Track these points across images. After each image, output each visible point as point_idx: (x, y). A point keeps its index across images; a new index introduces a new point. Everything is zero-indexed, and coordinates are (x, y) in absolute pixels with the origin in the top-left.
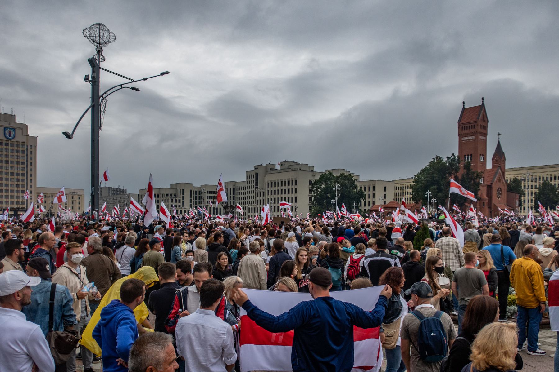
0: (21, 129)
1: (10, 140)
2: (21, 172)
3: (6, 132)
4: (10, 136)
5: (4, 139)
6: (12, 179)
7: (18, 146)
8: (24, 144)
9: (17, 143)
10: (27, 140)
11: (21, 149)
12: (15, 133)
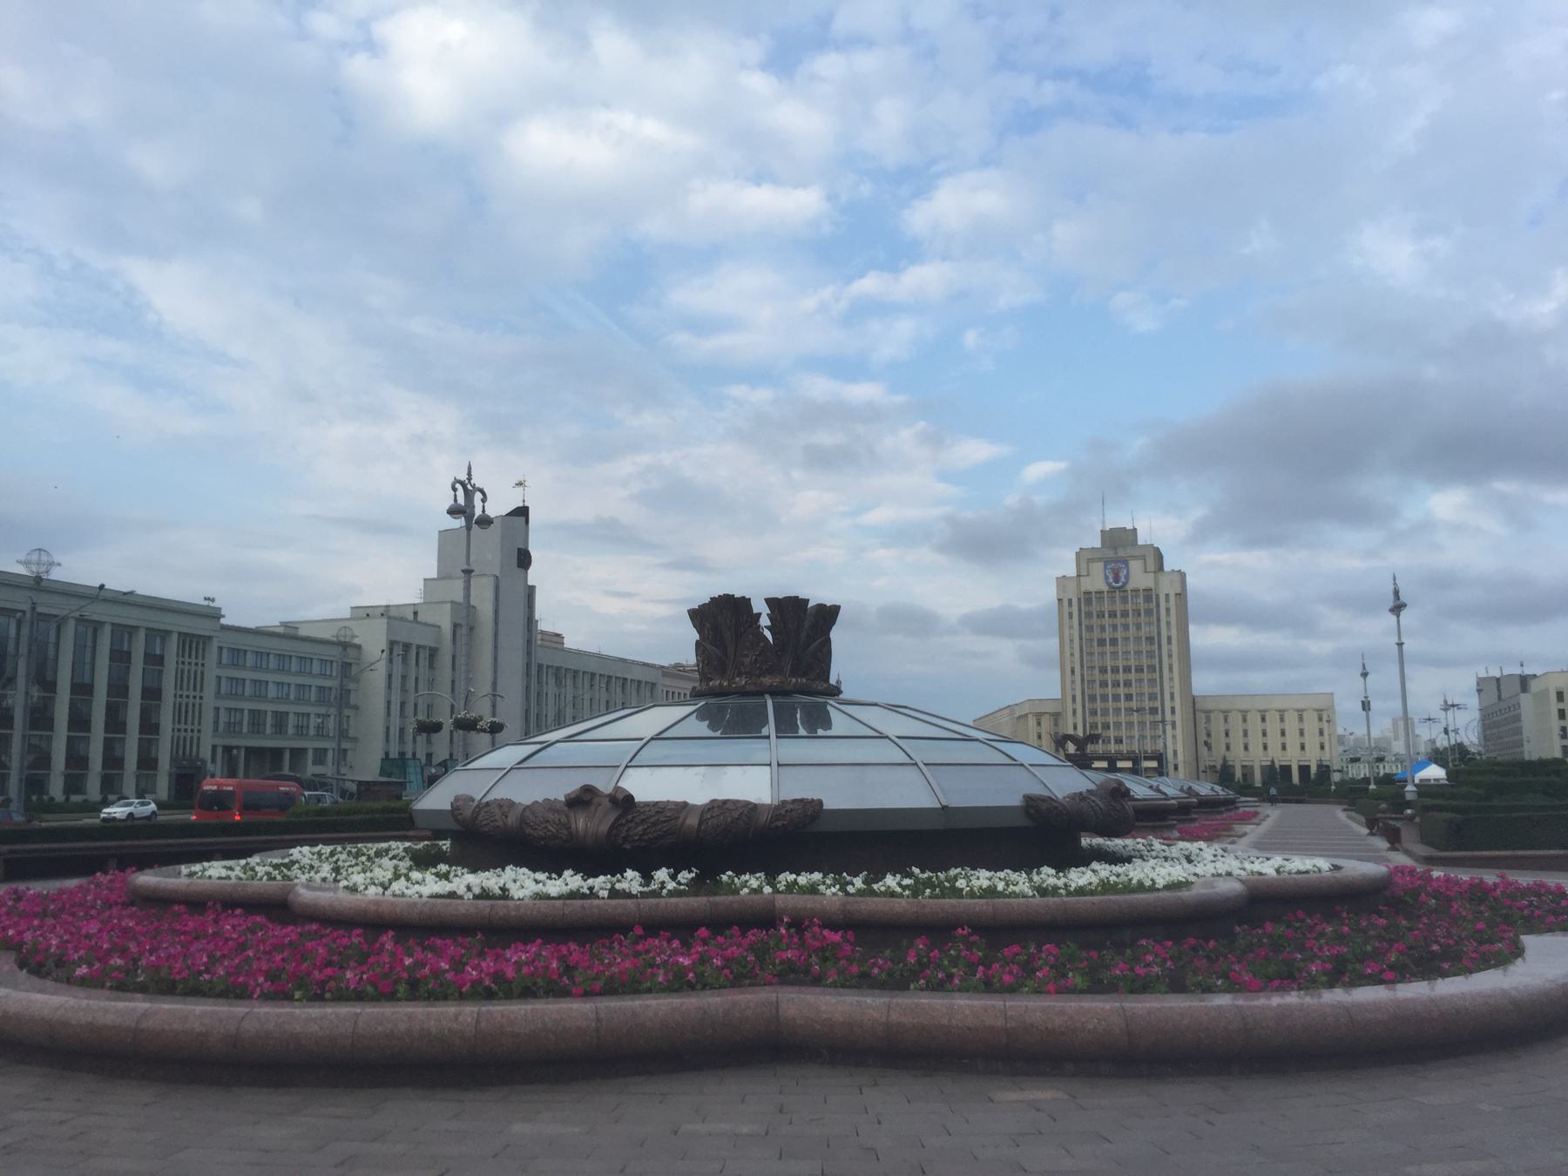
2: (1145, 662)
4: (1117, 579)
5: (1105, 588)
6: (1140, 681)
8: (1150, 593)
9: (1146, 593)
10: (1157, 582)
12: (1128, 571)
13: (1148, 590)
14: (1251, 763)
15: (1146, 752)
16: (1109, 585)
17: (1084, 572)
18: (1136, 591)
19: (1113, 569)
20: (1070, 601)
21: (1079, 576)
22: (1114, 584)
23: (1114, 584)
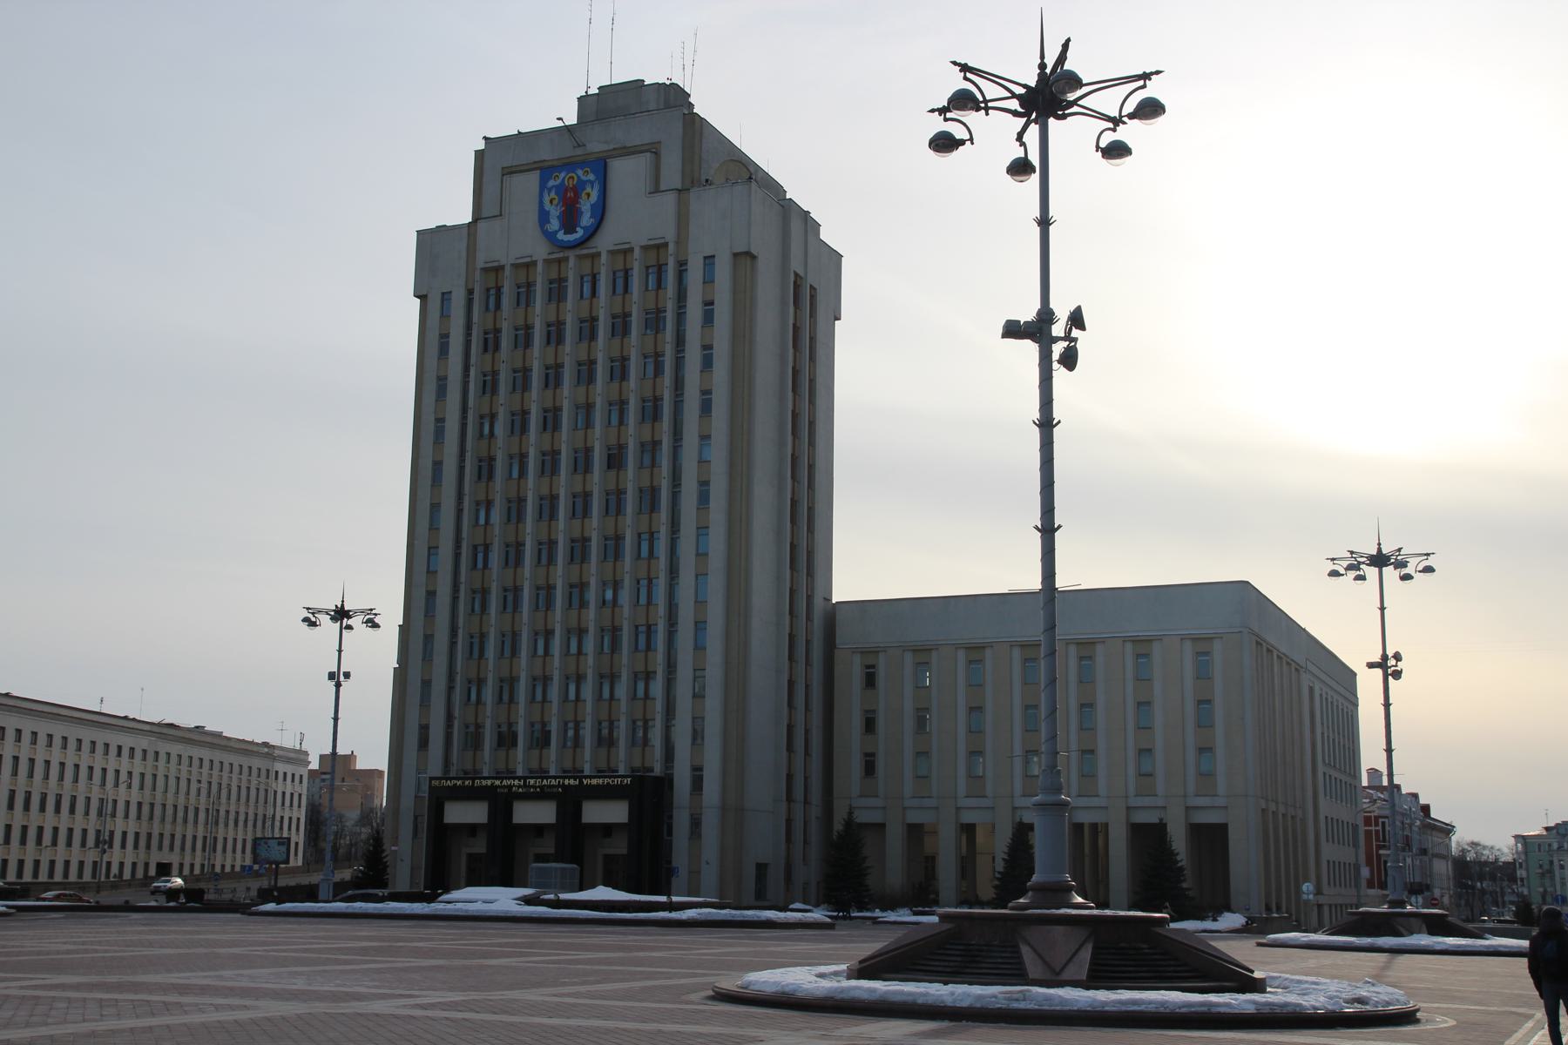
0: (654, 150)
1: (571, 254)
3: (547, 199)
4: (569, 223)
5: (540, 250)
10: (682, 220)
16: (550, 236)
17: (489, 209)
19: (562, 190)
20: (445, 297)
22: (561, 236)
23: (561, 236)
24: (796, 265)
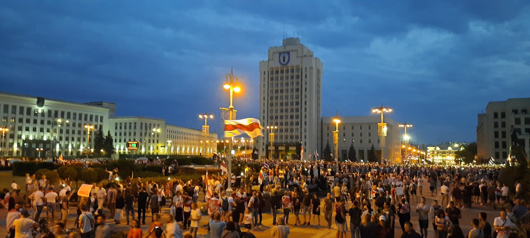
0: (297, 51)
3: (281, 57)
4: (284, 61)
5: (279, 65)
7: (292, 71)
11: (295, 74)
12: (289, 57)
13: (298, 66)
14: (346, 149)
15: (293, 143)
17: (271, 58)
18: (293, 67)
20: (265, 72)
21: (269, 60)
23: (283, 63)
24: (318, 67)
